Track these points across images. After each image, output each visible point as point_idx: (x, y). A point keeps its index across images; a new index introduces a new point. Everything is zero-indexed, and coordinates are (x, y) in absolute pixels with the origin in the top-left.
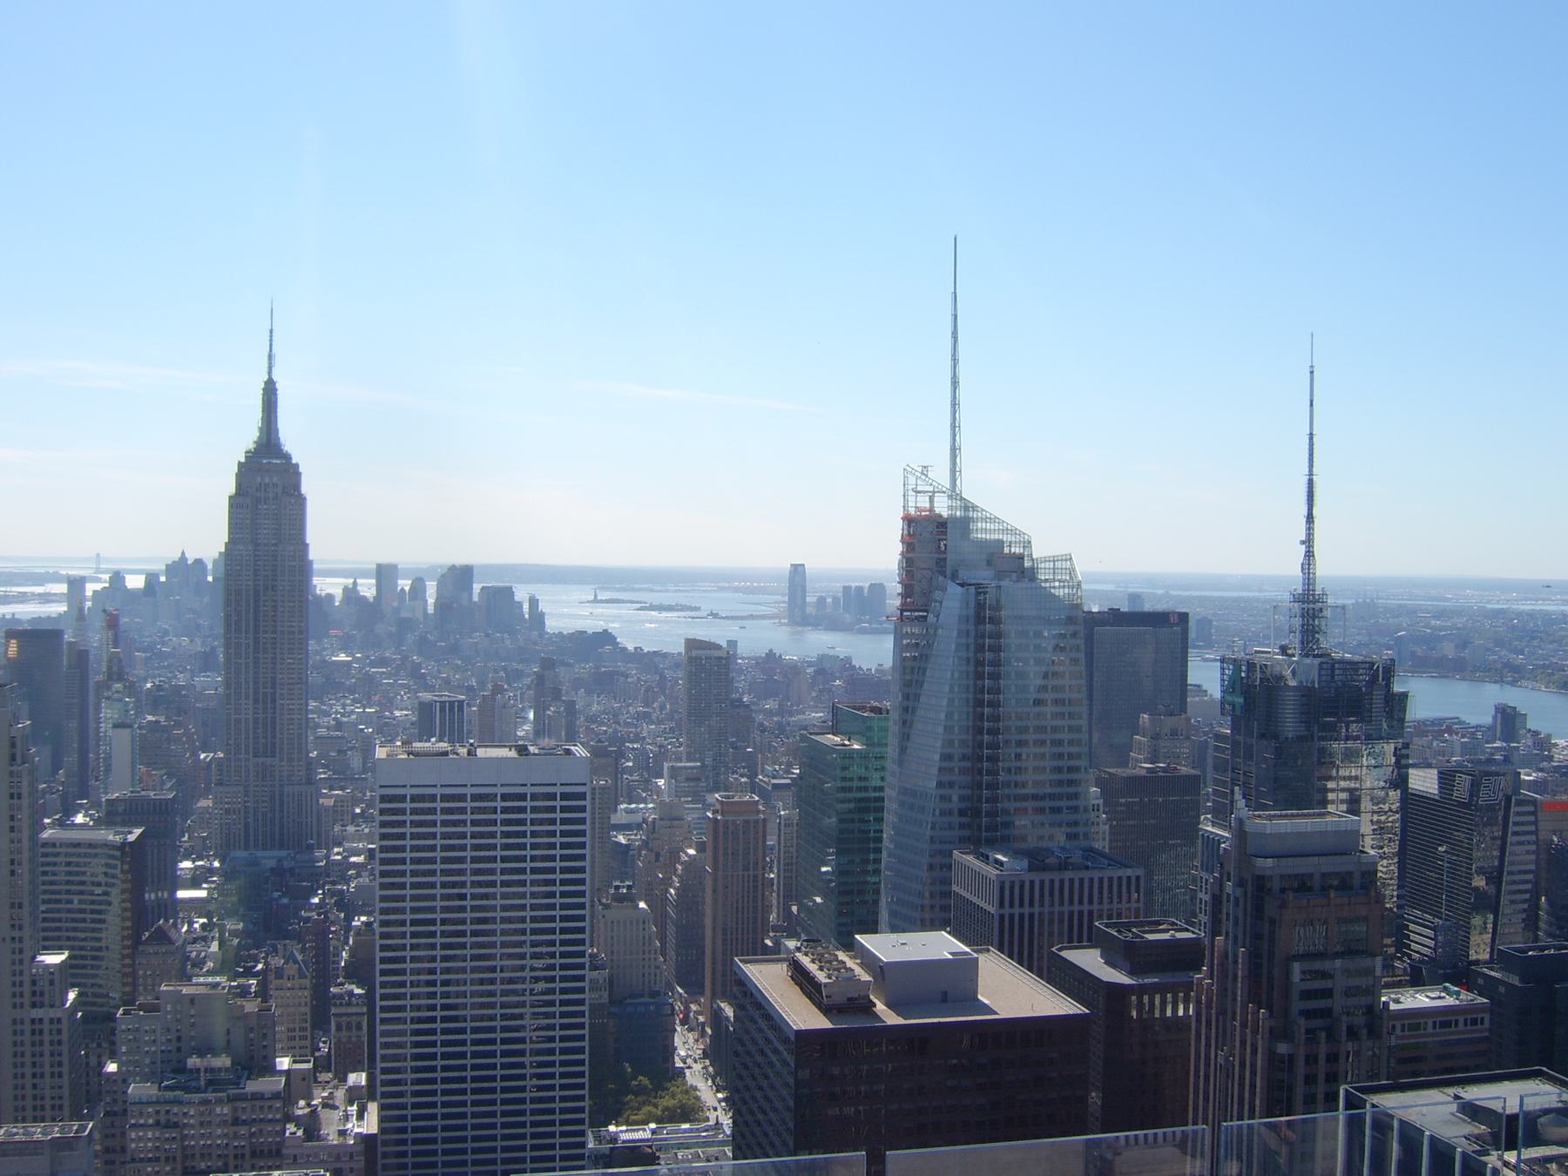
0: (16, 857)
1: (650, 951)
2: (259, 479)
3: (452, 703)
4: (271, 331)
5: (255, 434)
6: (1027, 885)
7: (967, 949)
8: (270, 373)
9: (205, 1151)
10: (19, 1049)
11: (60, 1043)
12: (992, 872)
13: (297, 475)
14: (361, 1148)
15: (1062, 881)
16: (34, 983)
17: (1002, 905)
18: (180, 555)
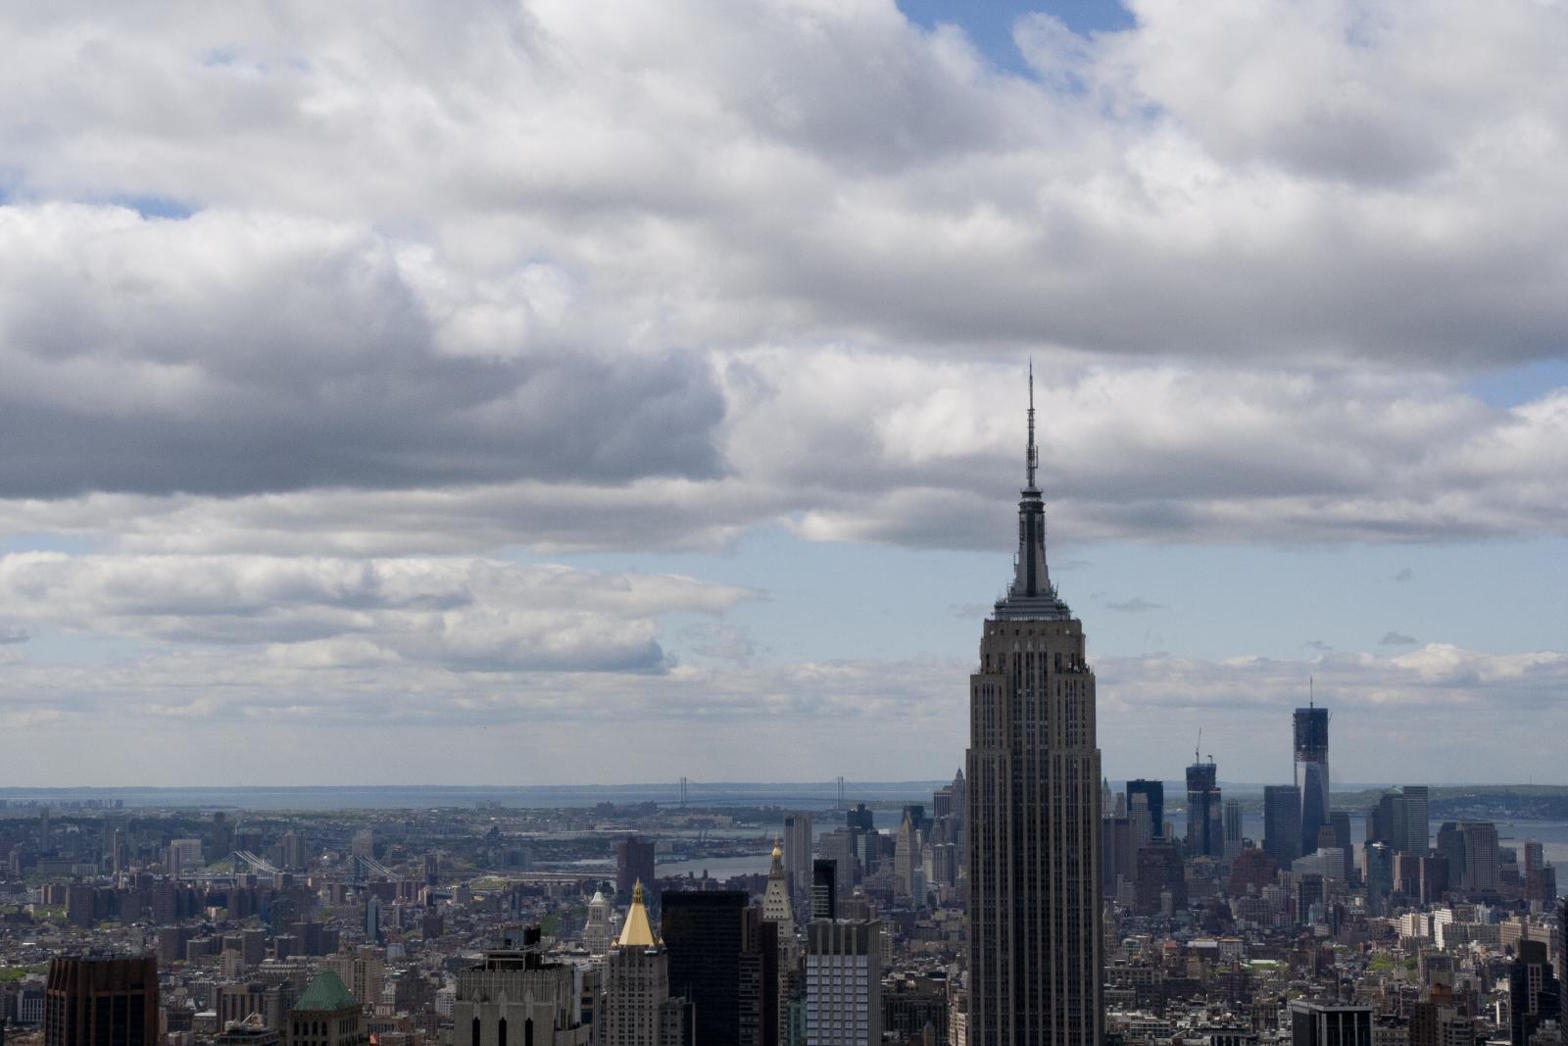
2: (1017, 646)
3: (1348, 1015)
4: (1031, 411)
5: (1014, 576)
8: (1031, 477)
13: (1078, 638)
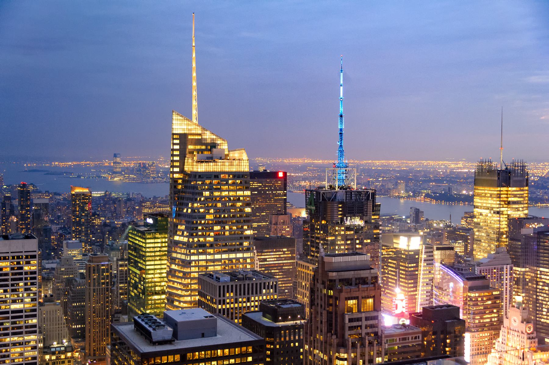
1: (61, 324)
6: (230, 287)
12: (215, 283)
15: (244, 285)
17: (220, 296)
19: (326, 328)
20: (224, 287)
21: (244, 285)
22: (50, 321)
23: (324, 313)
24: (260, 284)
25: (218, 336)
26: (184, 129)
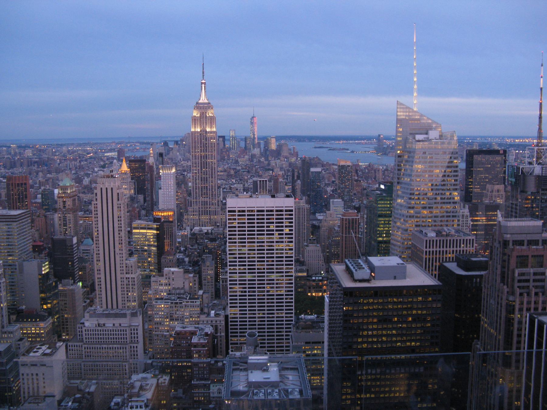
0: (120, 229)
6: (435, 241)
7: (402, 262)
9: (177, 318)
10: (123, 286)
11: (134, 285)
14: (224, 319)
15: (447, 240)
16: (126, 267)
17: (426, 248)
18: (184, 135)
19: (500, 279)
20: (430, 241)
21: (447, 240)
22: (313, 258)
23: (499, 267)
24: (460, 240)
25: (408, 279)
26: (406, 116)
